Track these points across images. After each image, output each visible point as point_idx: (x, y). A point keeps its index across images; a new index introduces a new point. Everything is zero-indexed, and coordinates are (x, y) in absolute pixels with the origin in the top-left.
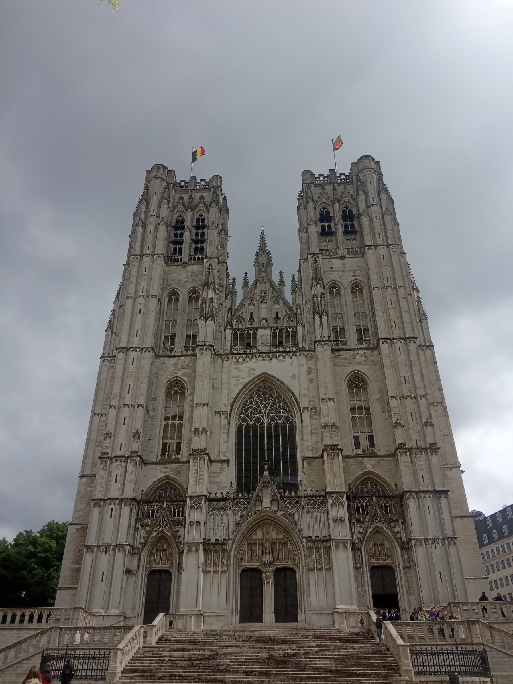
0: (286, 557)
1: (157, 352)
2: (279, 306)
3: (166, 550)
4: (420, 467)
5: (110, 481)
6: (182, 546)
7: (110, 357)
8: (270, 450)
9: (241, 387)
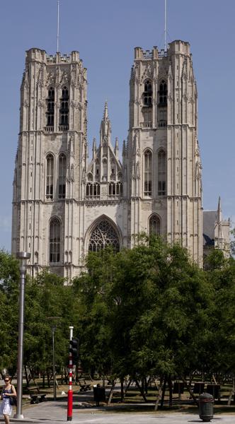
9: (90, 223)
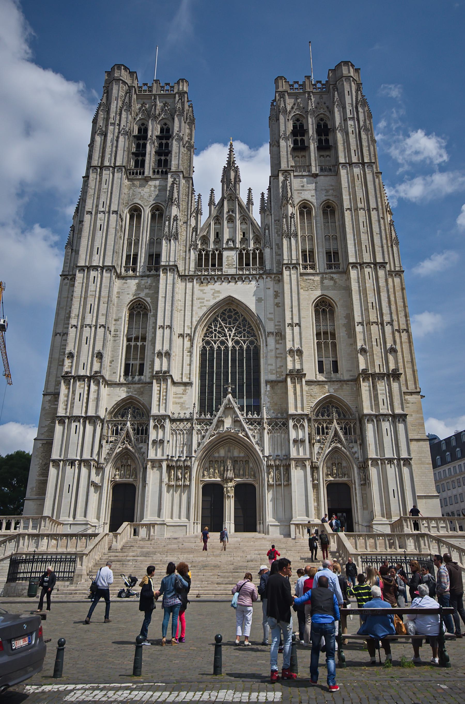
0: (247, 473)
1: (119, 272)
2: (246, 226)
3: (130, 466)
4: (381, 392)
5: (74, 399)
6: (145, 462)
7: (71, 275)
8: (233, 373)
9: (205, 309)
